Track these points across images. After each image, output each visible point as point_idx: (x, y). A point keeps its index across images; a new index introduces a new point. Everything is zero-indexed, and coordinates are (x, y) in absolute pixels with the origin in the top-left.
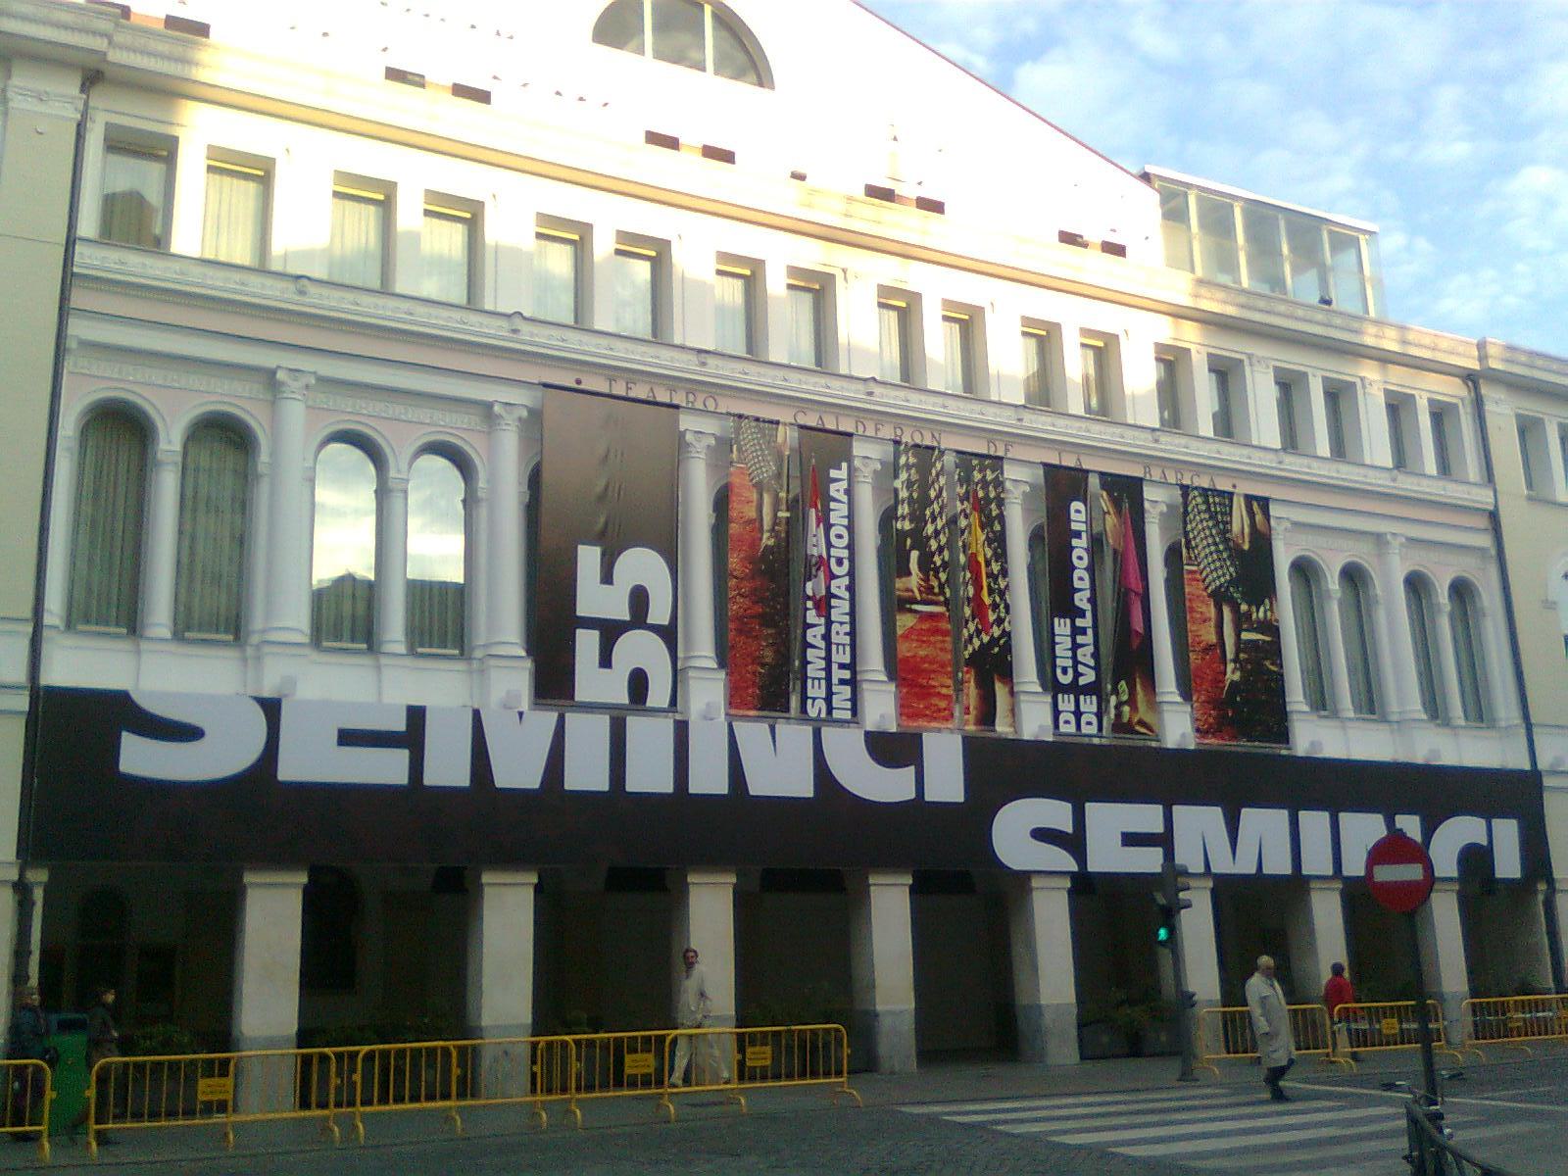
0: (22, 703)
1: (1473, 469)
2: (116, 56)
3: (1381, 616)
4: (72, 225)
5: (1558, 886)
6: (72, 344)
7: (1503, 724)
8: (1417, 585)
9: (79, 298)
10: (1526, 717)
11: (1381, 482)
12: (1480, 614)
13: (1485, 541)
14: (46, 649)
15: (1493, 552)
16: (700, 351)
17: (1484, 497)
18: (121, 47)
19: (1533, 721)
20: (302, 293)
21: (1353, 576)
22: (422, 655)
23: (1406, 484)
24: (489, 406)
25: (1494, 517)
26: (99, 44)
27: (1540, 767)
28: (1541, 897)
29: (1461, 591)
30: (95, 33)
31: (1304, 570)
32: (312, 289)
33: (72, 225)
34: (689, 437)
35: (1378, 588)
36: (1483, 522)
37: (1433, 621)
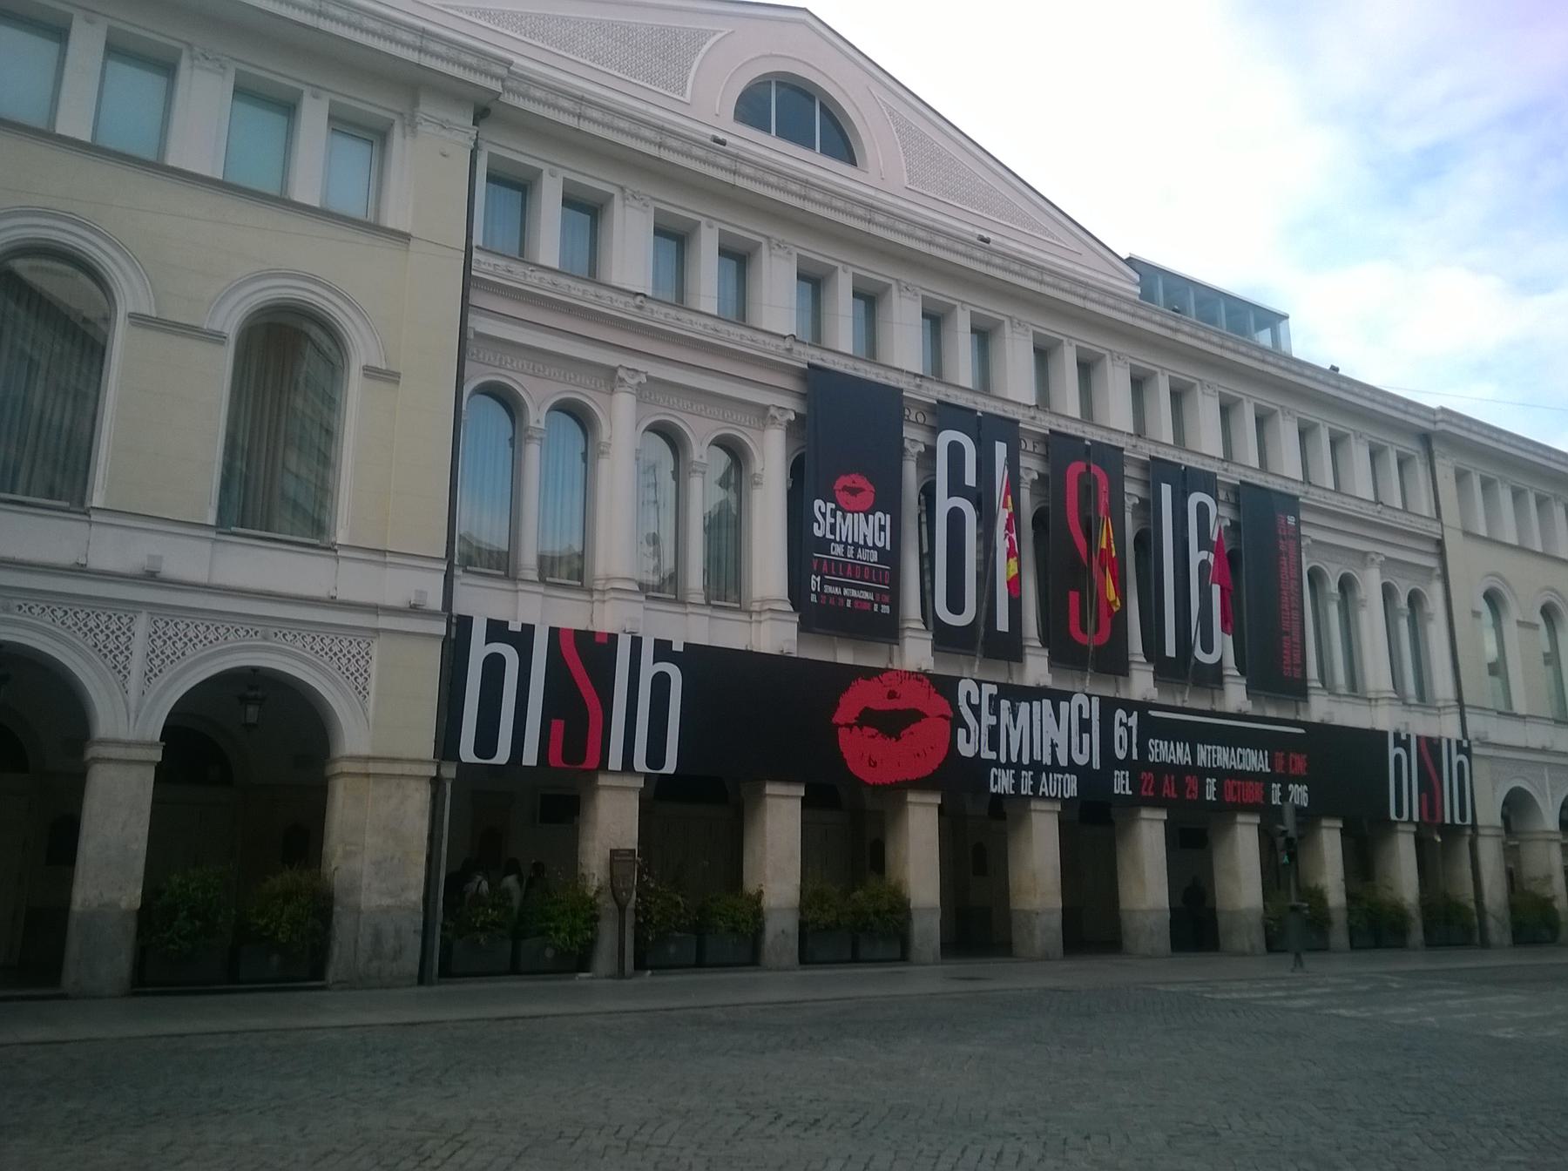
0: (440, 628)
1: (1426, 508)
2: (509, 99)
3: (1363, 616)
4: (469, 236)
5: (1481, 831)
6: (471, 335)
7: (1440, 704)
8: (1388, 592)
9: (477, 298)
10: (1460, 699)
11: (1369, 512)
12: (1430, 617)
13: (1432, 562)
14: (456, 583)
15: (1439, 571)
16: (916, 375)
17: (1434, 529)
18: (510, 90)
19: (1466, 702)
20: (640, 308)
21: (1346, 584)
22: (715, 606)
23: (1388, 517)
24: (767, 408)
25: (1440, 543)
26: (496, 86)
27: (1471, 736)
28: (1467, 839)
29: (1415, 599)
30: (494, 77)
31: (1316, 576)
32: (648, 305)
33: (469, 236)
34: (907, 444)
35: (1362, 593)
36: (1431, 548)
37: (1396, 623)
